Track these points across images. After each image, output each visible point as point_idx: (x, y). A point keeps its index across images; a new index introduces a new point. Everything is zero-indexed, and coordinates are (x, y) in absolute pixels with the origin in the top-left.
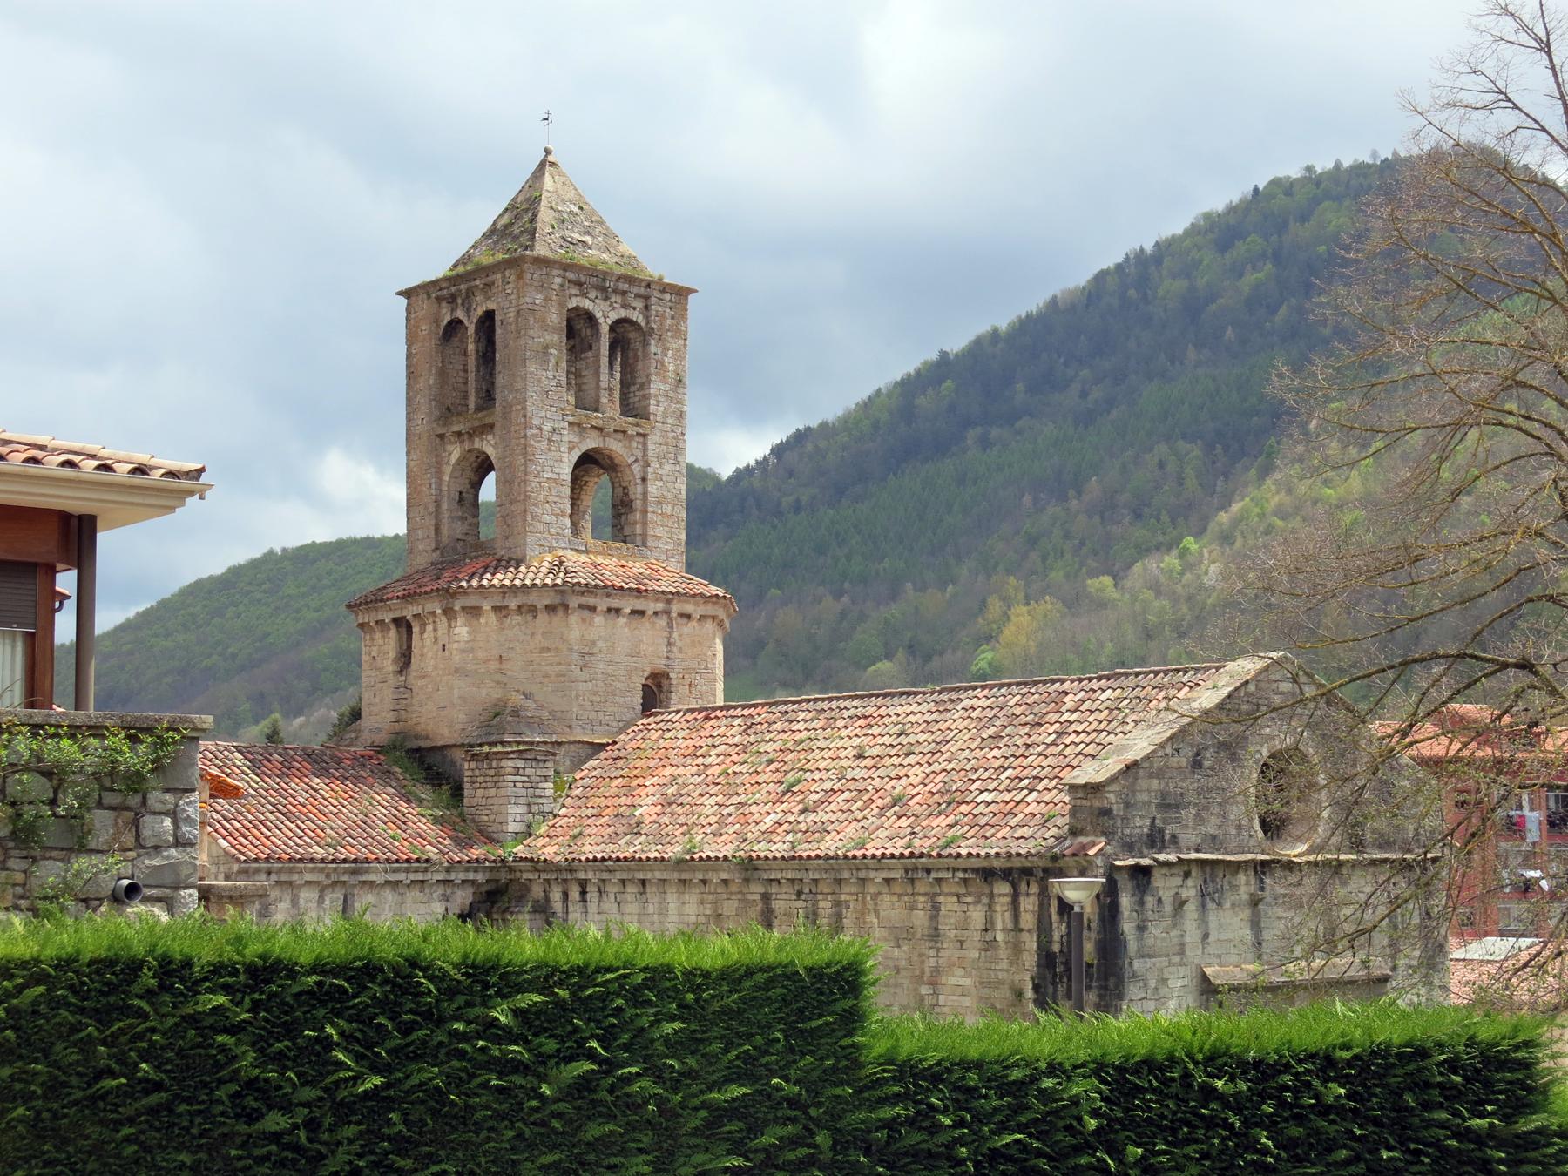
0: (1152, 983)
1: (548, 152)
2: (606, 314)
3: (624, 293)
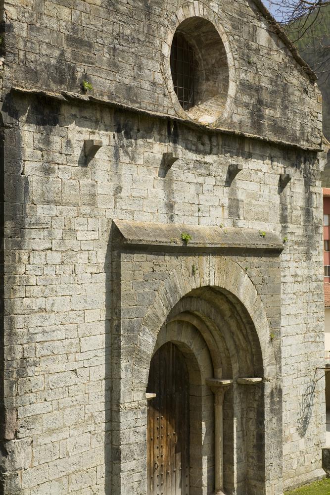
0: (58, 233)
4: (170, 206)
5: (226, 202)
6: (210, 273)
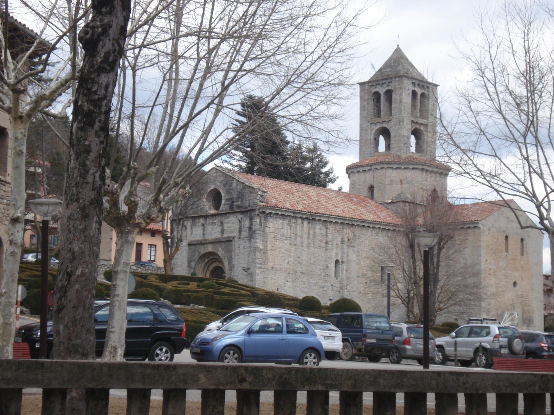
1: (398, 46)
2: (382, 90)
3: (385, 83)
4: (204, 235)
5: (220, 230)
6: (210, 249)
